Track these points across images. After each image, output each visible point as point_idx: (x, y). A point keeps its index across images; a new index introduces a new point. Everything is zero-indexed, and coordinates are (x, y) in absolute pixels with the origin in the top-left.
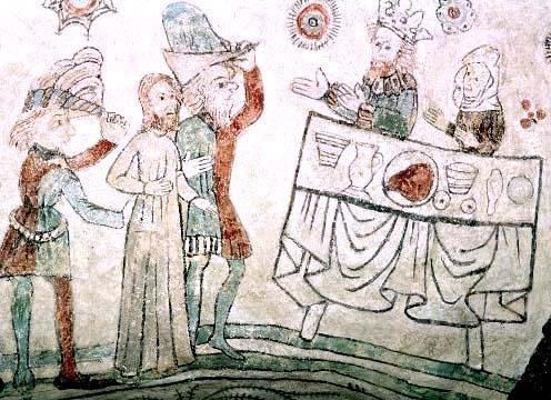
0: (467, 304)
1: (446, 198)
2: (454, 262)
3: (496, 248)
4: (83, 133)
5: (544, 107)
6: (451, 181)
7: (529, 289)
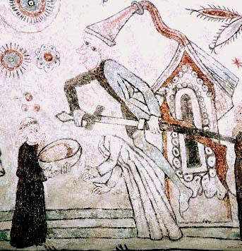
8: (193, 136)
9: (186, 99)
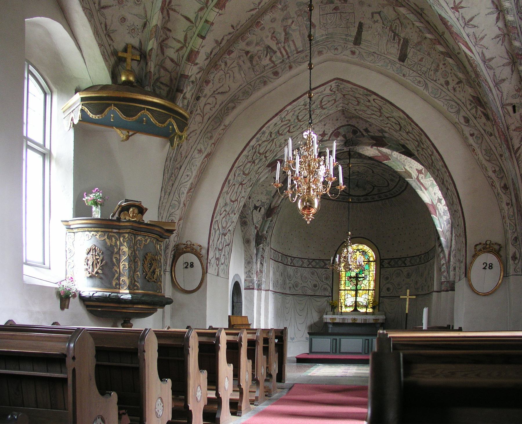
4: (290, 21)
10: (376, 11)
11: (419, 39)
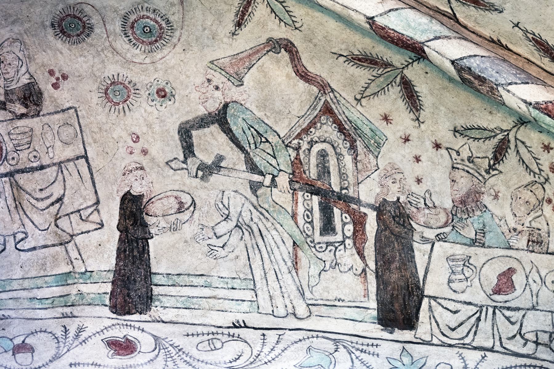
0: (58, 227)
1: (15, 155)
2: (37, 199)
3: (64, 181)
5: (66, 70)
6: (16, 142)
7: (98, 202)
8: (329, 200)
9: (323, 155)
10: (202, 111)
11: (464, 183)
